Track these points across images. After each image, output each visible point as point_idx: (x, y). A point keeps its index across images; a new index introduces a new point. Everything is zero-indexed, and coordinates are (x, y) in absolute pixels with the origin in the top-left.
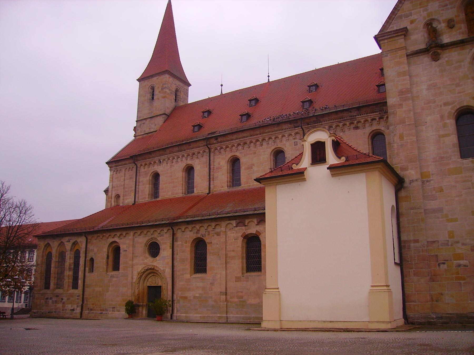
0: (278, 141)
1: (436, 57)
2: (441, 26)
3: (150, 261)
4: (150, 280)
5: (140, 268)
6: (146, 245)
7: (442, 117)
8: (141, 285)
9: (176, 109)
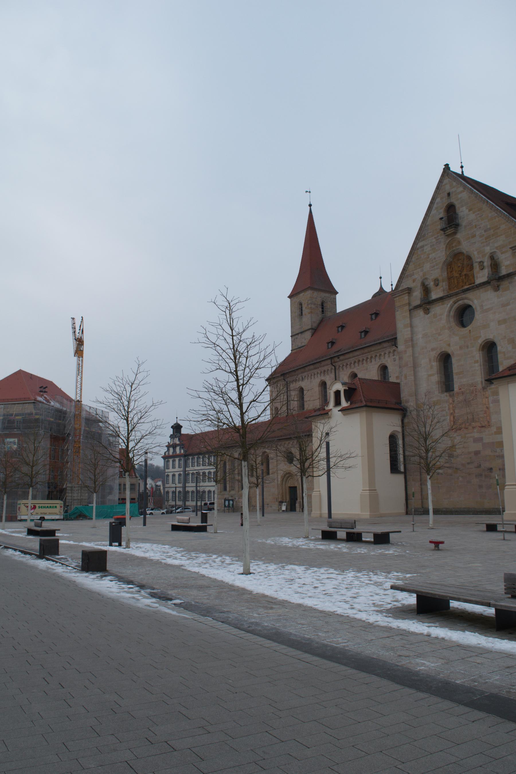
0: (382, 358)
1: (427, 311)
2: (431, 284)
5: (281, 473)
7: (430, 360)
9: (321, 321)
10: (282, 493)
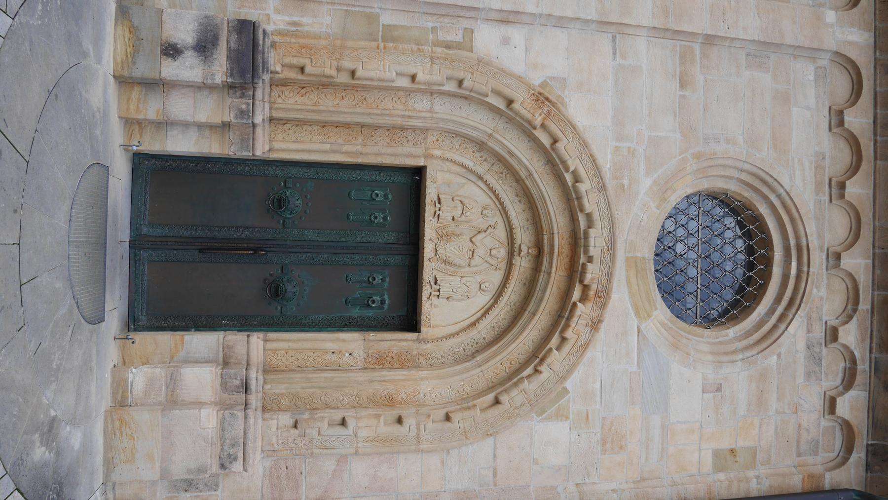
3: (632, 220)
4: (476, 194)
6: (764, 182)
8: (444, 109)
10: (355, 85)
